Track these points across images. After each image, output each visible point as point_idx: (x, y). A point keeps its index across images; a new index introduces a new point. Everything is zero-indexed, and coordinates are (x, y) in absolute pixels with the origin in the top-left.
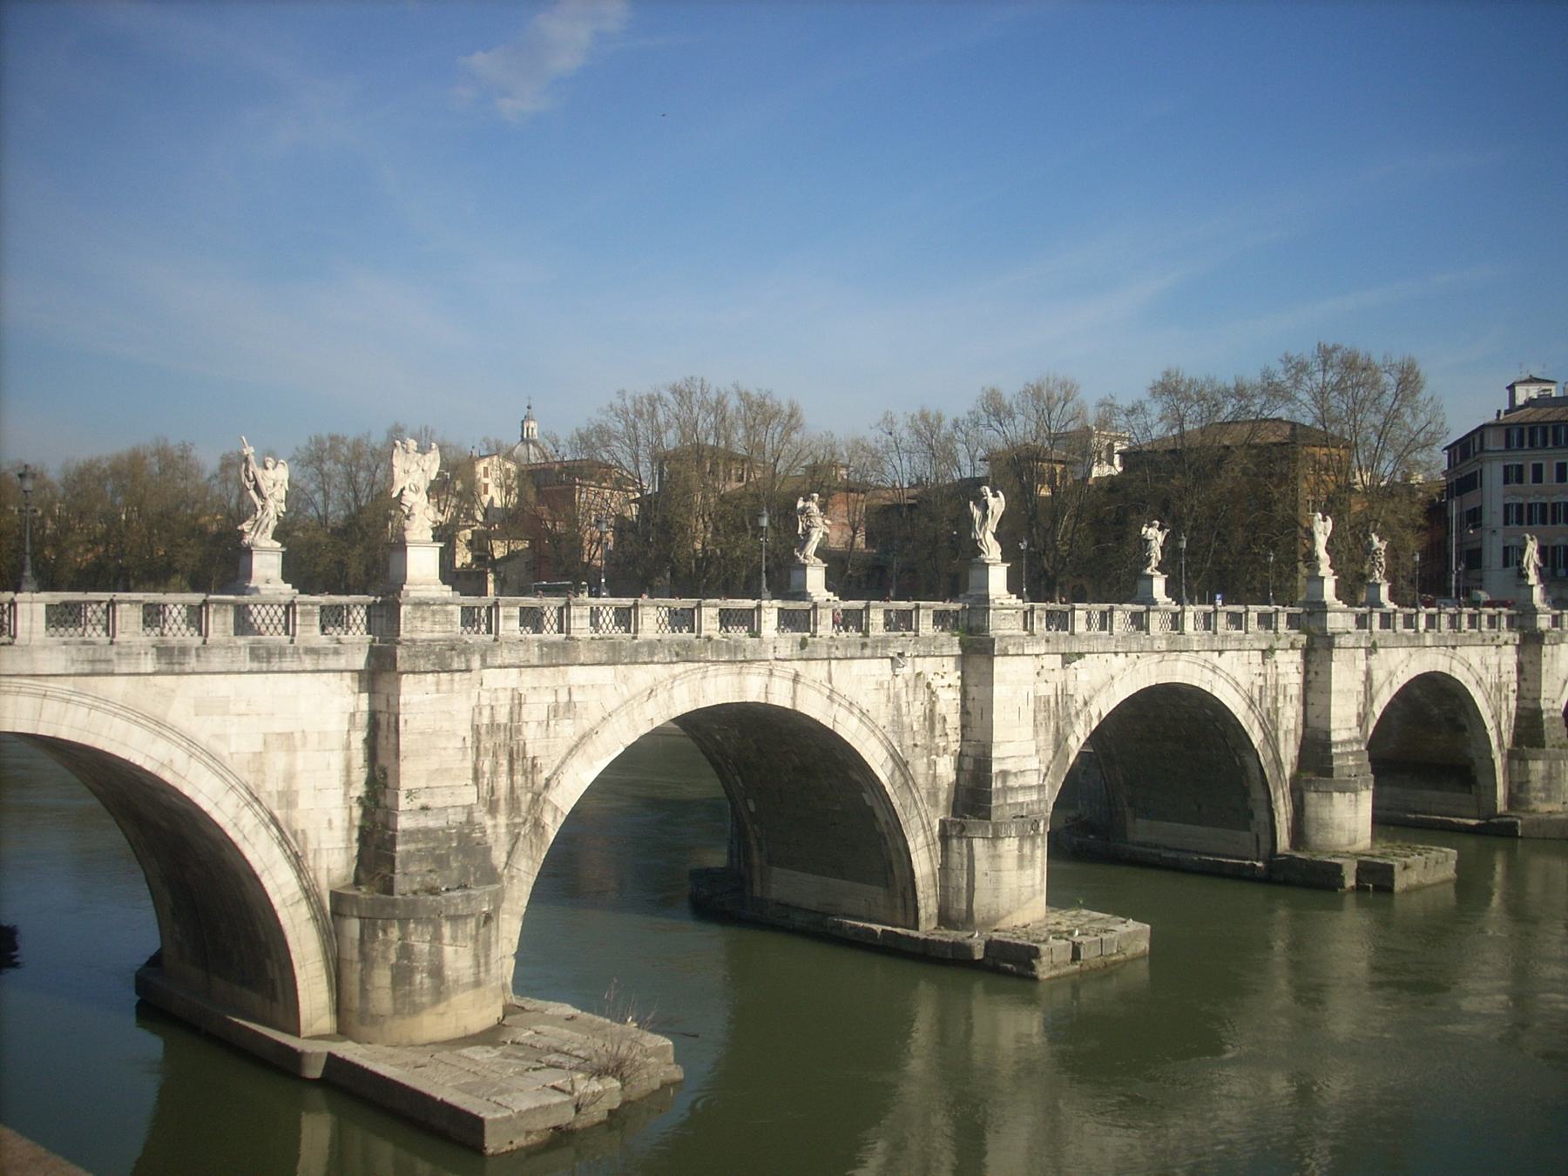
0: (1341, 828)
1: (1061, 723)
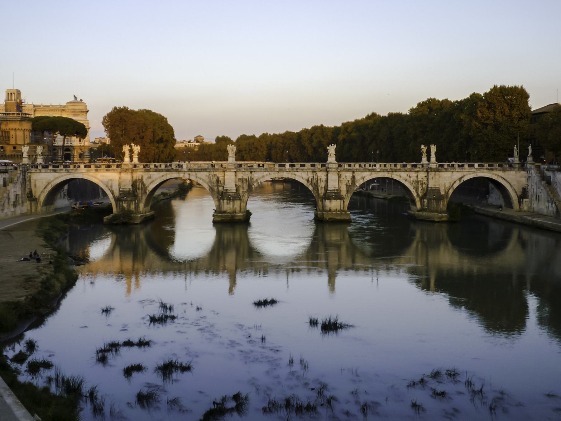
0: (328, 207)
1: (250, 183)
